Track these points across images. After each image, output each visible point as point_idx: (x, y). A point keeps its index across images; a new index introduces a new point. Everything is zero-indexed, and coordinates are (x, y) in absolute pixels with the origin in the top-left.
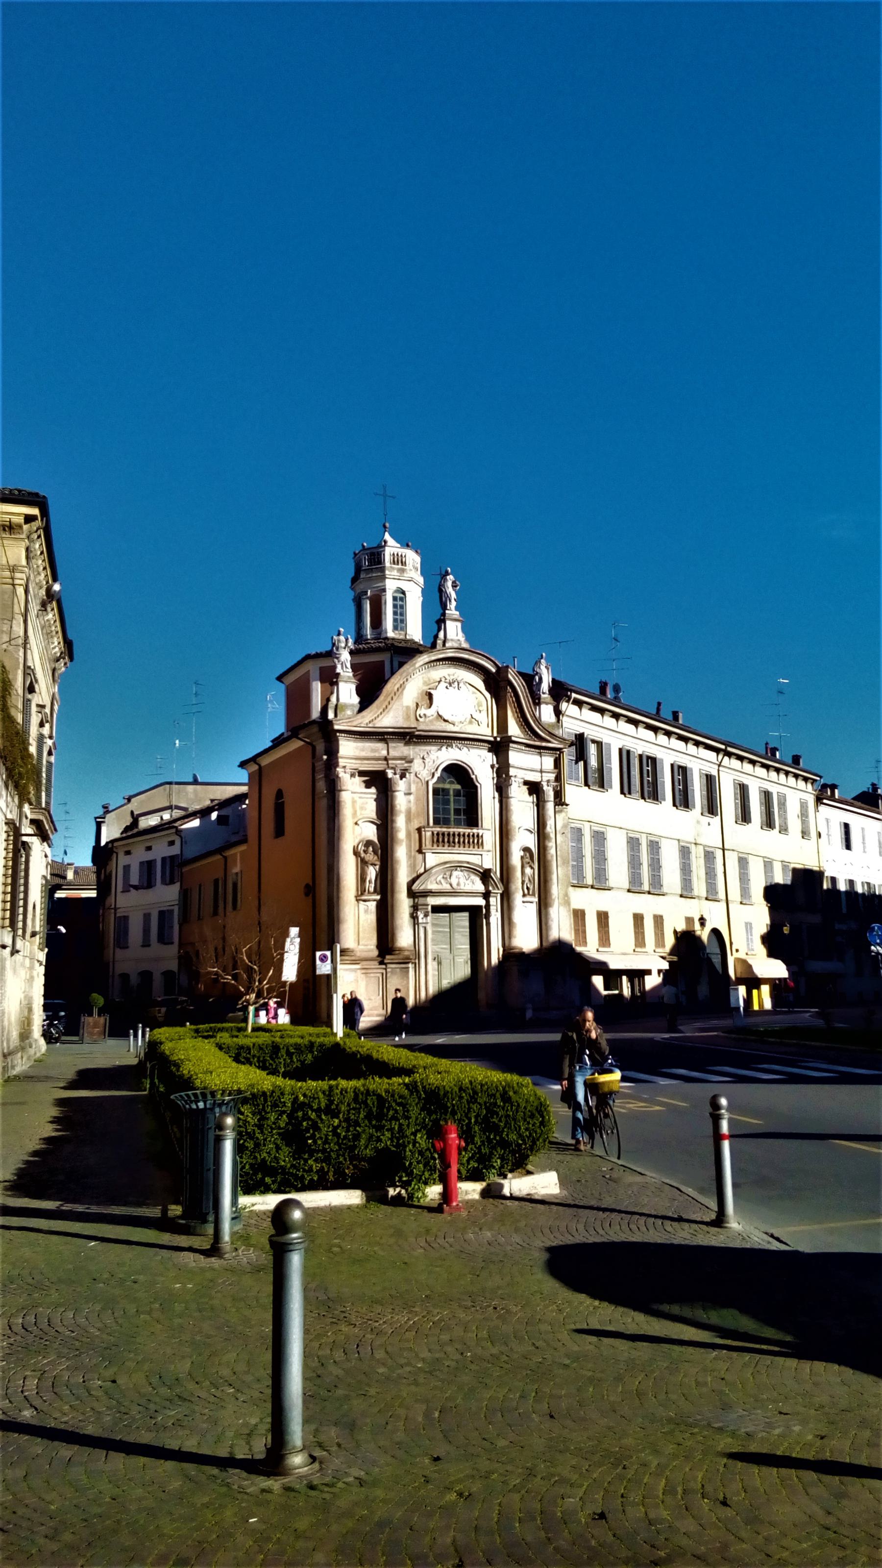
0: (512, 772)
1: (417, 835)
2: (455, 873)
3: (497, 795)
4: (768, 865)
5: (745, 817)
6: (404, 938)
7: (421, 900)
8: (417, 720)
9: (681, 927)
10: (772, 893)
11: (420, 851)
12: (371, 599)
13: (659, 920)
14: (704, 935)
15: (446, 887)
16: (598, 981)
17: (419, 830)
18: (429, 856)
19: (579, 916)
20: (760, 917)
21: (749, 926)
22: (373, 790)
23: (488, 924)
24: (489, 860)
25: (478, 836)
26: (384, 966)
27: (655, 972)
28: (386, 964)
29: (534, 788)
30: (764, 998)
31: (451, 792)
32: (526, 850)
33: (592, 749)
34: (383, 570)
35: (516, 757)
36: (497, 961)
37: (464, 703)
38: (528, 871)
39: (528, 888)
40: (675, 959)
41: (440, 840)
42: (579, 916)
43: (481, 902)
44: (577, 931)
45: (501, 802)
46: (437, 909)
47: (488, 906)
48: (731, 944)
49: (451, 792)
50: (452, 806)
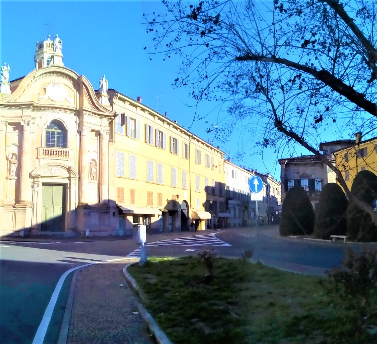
0: (85, 124)
1: (36, 151)
2: (53, 168)
3: (78, 135)
4: (206, 179)
5: (199, 162)
6: (26, 195)
7: (36, 180)
8: (39, 100)
9: (170, 198)
10: (207, 189)
11: (37, 158)
12: (38, 63)
13: (160, 196)
14: (180, 201)
15: (50, 175)
16: (130, 219)
17: (37, 149)
18: (41, 160)
19: (120, 191)
20: (203, 197)
21: (198, 200)
22: (17, 131)
23: (70, 191)
24: (74, 165)
25: (66, 152)
26: (15, 208)
27: (156, 216)
28: (15, 207)
29: (98, 134)
30: (202, 226)
31: (56, 133)
32: (93, 160)
33: (130, 123)
34: (43, 50)
35: (87, 117)
36: (74, 209)
37: (63, 92)
38: (93, 169)
39: (93, 177)
40: (166, 211)
41: (47, 153)
42: (120, 191)
43: (67, 181)
44: (119, 197)
45: (80, 138)
46: (44, 184)
47: (70, 184)
48: (191, 206)
49: (56, 133)
50: (56, 139)
